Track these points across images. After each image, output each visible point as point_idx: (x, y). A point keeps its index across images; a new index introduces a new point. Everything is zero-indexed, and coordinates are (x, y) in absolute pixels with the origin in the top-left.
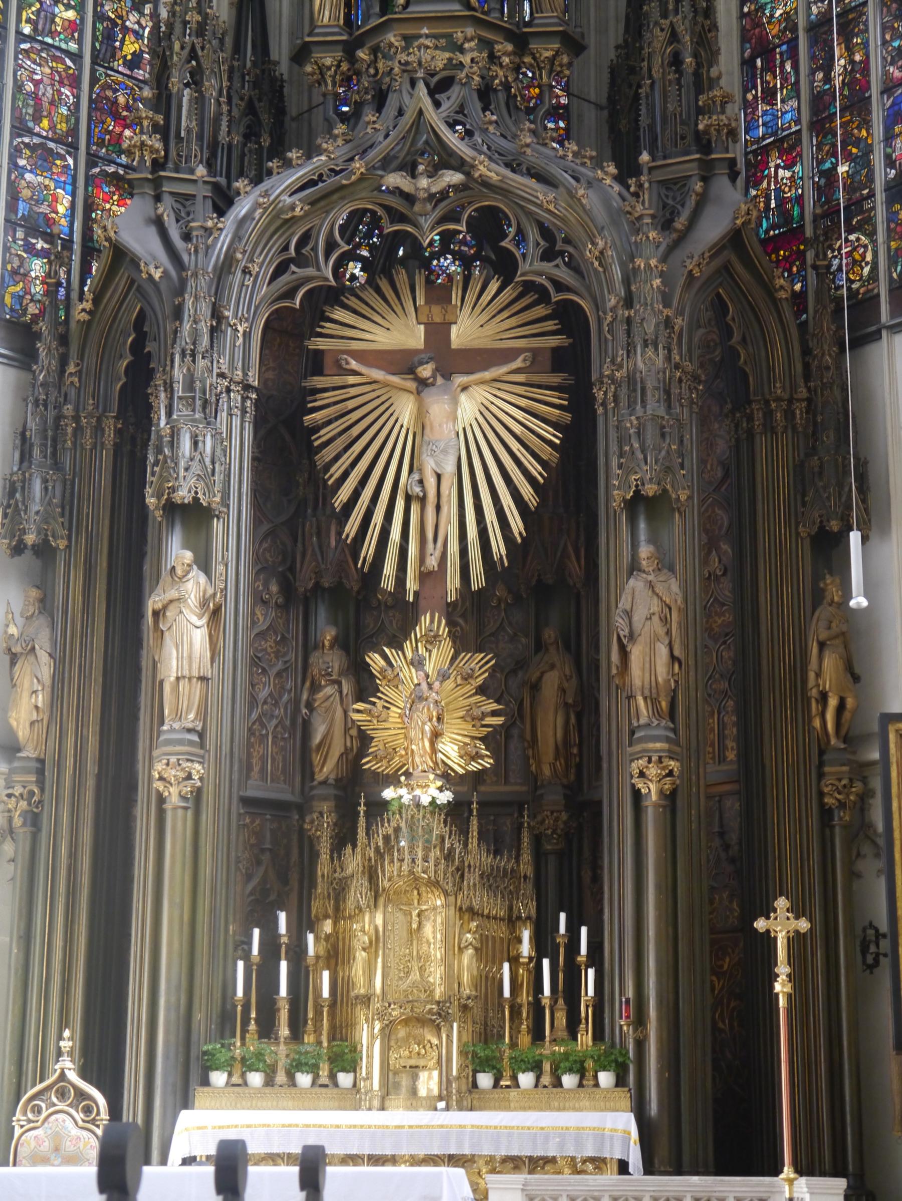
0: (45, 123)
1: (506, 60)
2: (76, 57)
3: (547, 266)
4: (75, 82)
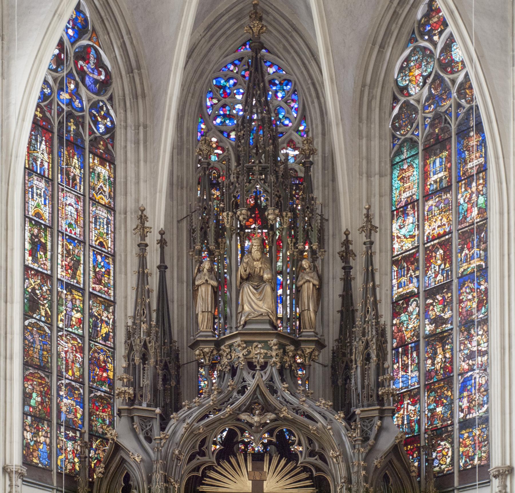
0: (70, 372)
1: (291, 354)
2: (82, 337)
3: (312, 460)
4: (81, 350)
